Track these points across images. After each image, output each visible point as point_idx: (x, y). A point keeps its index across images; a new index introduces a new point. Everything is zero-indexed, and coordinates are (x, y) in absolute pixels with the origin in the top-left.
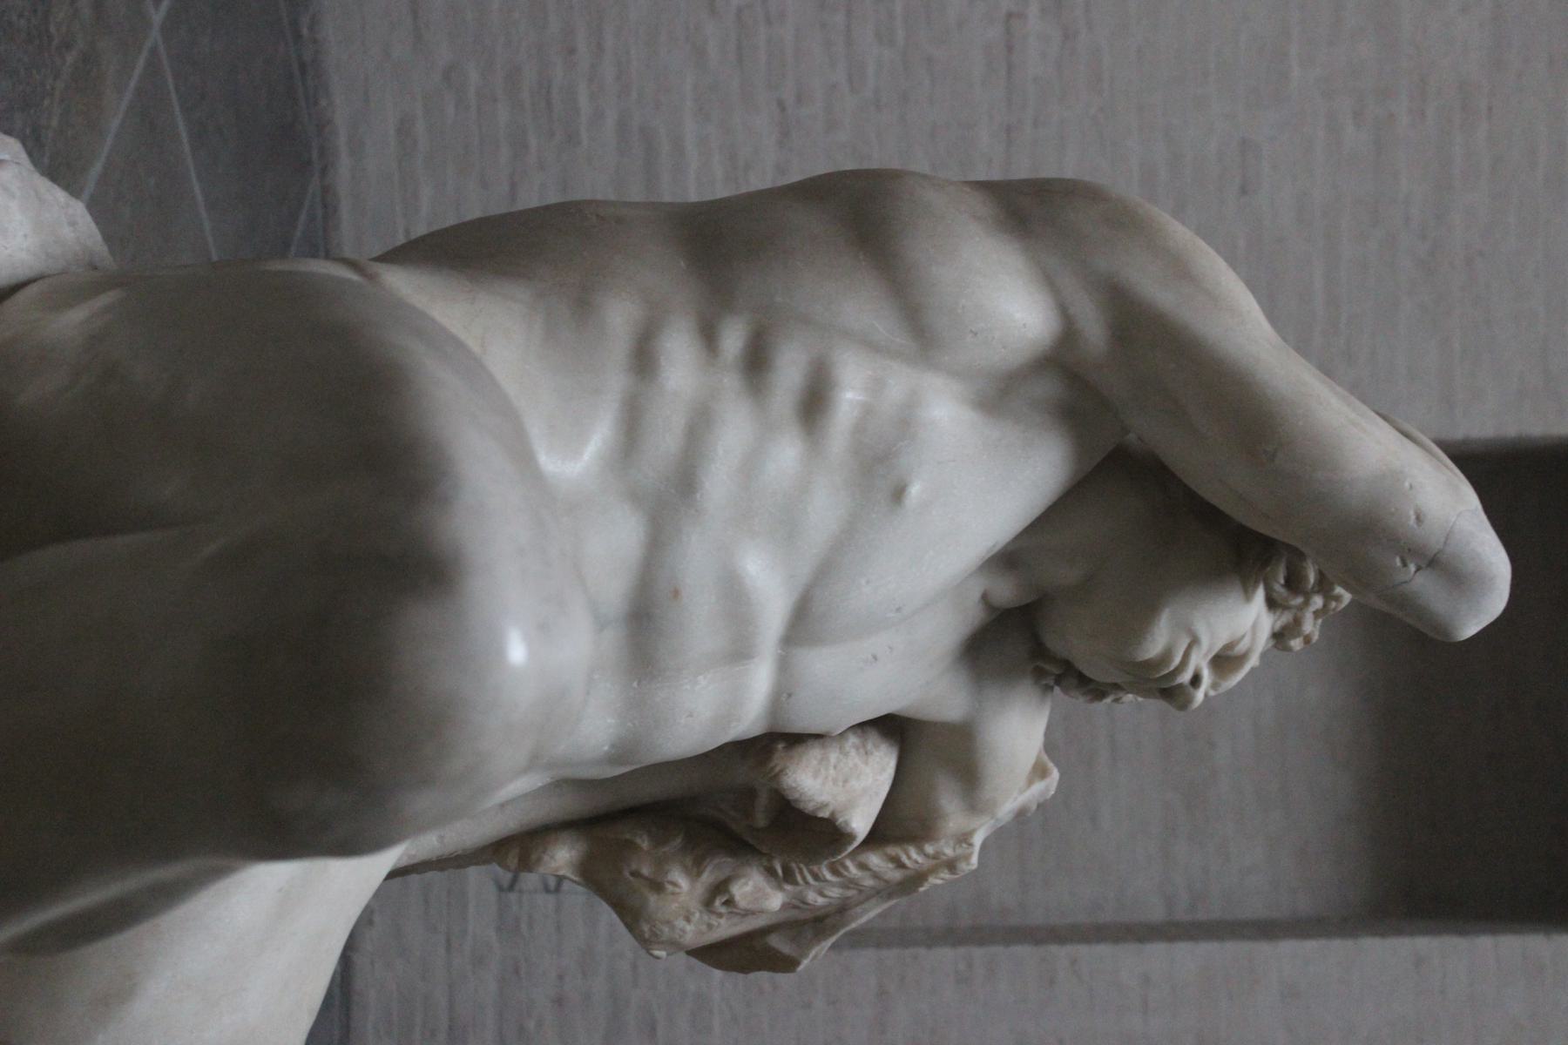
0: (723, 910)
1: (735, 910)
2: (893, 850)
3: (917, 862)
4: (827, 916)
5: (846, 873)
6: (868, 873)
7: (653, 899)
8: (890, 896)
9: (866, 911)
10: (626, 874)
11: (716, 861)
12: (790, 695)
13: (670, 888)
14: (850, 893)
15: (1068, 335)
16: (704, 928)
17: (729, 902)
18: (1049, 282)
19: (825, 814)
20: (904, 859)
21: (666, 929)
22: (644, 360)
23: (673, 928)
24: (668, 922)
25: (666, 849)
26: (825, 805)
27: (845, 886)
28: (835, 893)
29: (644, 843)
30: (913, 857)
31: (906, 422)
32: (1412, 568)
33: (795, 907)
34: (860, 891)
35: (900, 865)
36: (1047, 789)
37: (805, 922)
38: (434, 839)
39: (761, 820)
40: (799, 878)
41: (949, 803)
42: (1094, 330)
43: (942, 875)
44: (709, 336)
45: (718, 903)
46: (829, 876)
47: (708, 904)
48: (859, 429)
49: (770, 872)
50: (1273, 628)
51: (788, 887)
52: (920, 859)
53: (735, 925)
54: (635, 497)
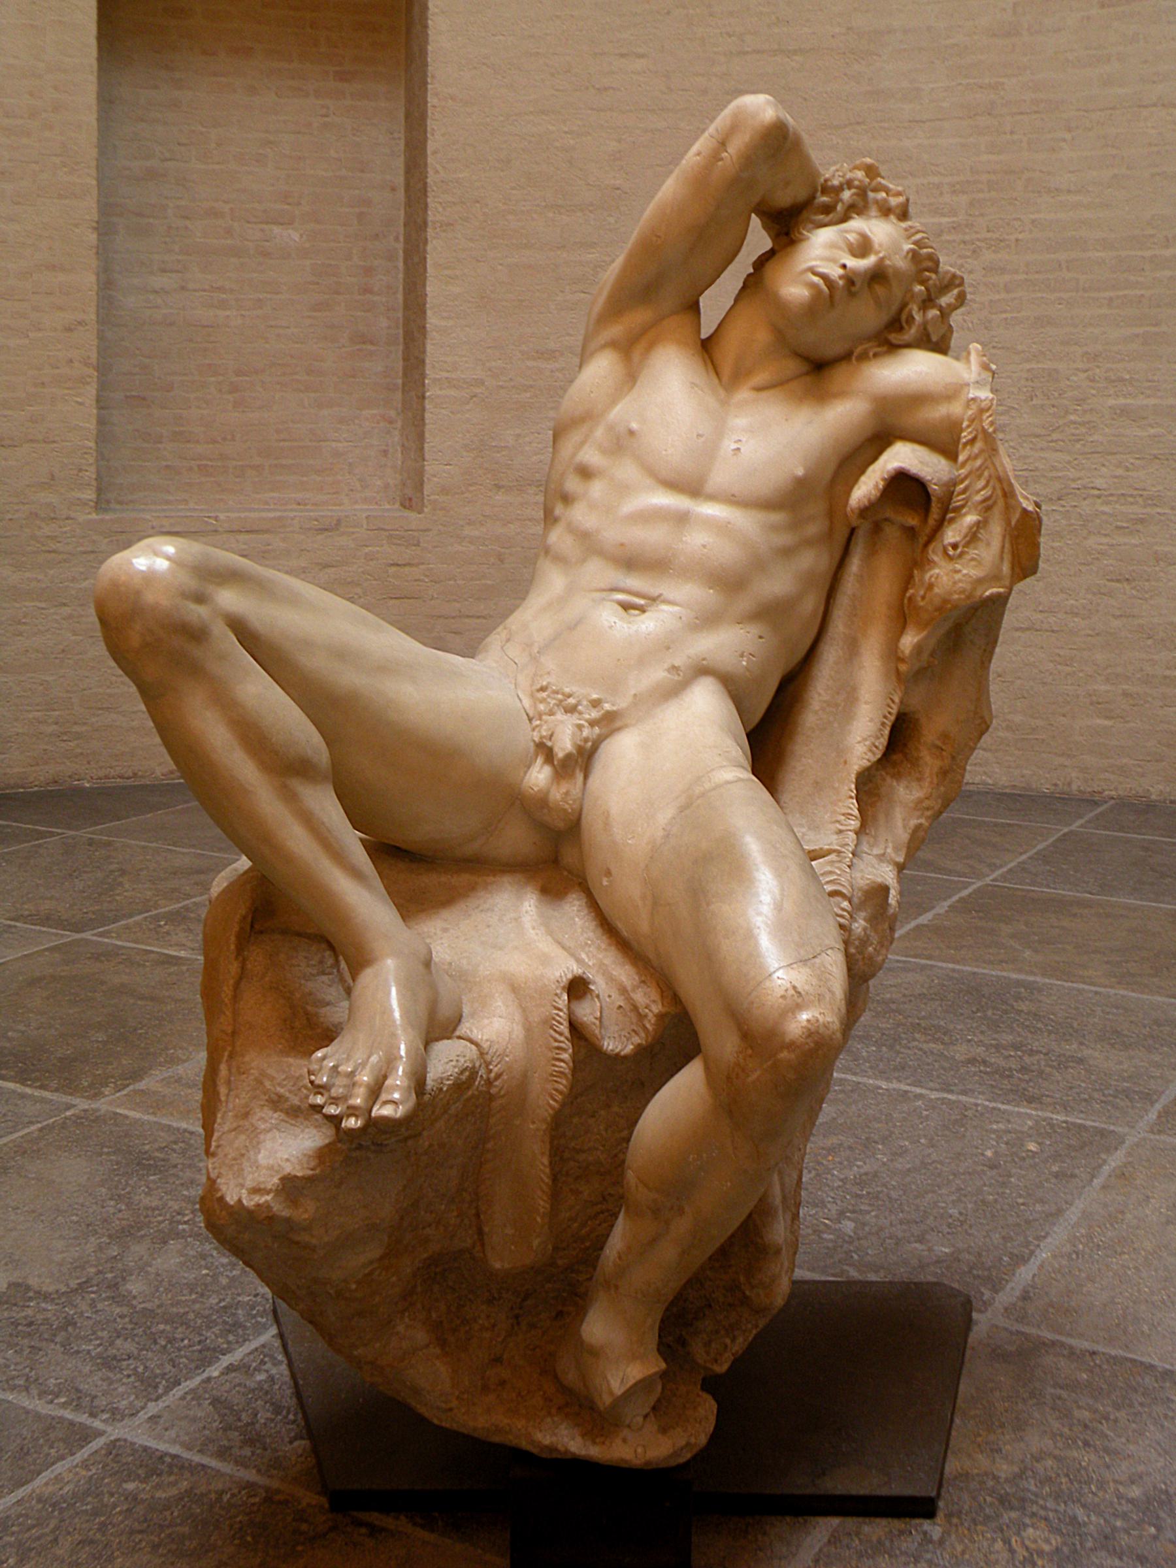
0: (959, 550)
1: (963, 542)
2: (960, 446)
3: (971, 432)
4: (1003, 489)
5: (963, 476)
6: (970, 462)
7: (936, 590)
8: (995, 450)
9: (1002, 464)
10: (922, 604)
11: (930, 552)
12: (733, 495)
13: (933, 579)
14: (986, 474)
15: (613, 344)
16: (973, 563)
17: (955, 546)
18: (592, 354)
19: (881, 485)
20: (964, 440)
21: (961, 585)
22: (547, 551)
23: (960, 581)
24: (955, 583)
25: (917, 579)
26: (876, 485)
27: (979, 477)
28: (981, 483)
29: (911, 591)
30: (966, 436)
31: (611, 428)
32: (725, 155)
33: (988, 509)
34: (987, 468)
35: (972, 441)
36: (977, 350)
37: (1006, 503)
38: (864, 706)
39: (912, 521)
40: (958, 504)
41: (940, 411)
42: (615, 330)
43: (984, 417)
44: (556, 520)
45: (951, 552)
46: (962, 486)
47: (951, 558)
48: (604, 451)
49: (952, 520)
50: (876, 217)
51: (964, 511)
52: (969, 430)
53: (988, 544)
54: (584, 560)
